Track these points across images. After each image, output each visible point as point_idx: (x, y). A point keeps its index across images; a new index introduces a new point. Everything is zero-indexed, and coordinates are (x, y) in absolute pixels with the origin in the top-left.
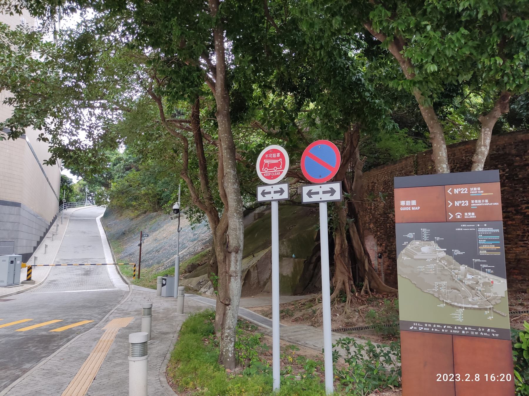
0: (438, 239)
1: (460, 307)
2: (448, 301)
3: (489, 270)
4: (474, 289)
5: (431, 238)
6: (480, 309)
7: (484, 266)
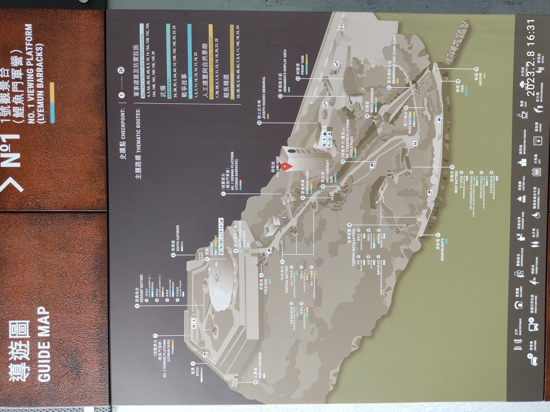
0: (176, 247)
1: (445, 178)
2: (423, 220)
3: (300, 69)
4: (373, 129)
5: (177, 273)
6: (448, 111)
7: (283, 86)
